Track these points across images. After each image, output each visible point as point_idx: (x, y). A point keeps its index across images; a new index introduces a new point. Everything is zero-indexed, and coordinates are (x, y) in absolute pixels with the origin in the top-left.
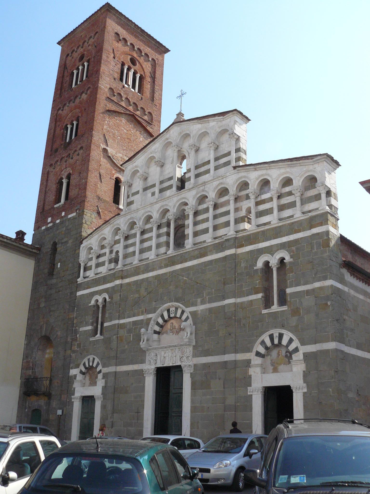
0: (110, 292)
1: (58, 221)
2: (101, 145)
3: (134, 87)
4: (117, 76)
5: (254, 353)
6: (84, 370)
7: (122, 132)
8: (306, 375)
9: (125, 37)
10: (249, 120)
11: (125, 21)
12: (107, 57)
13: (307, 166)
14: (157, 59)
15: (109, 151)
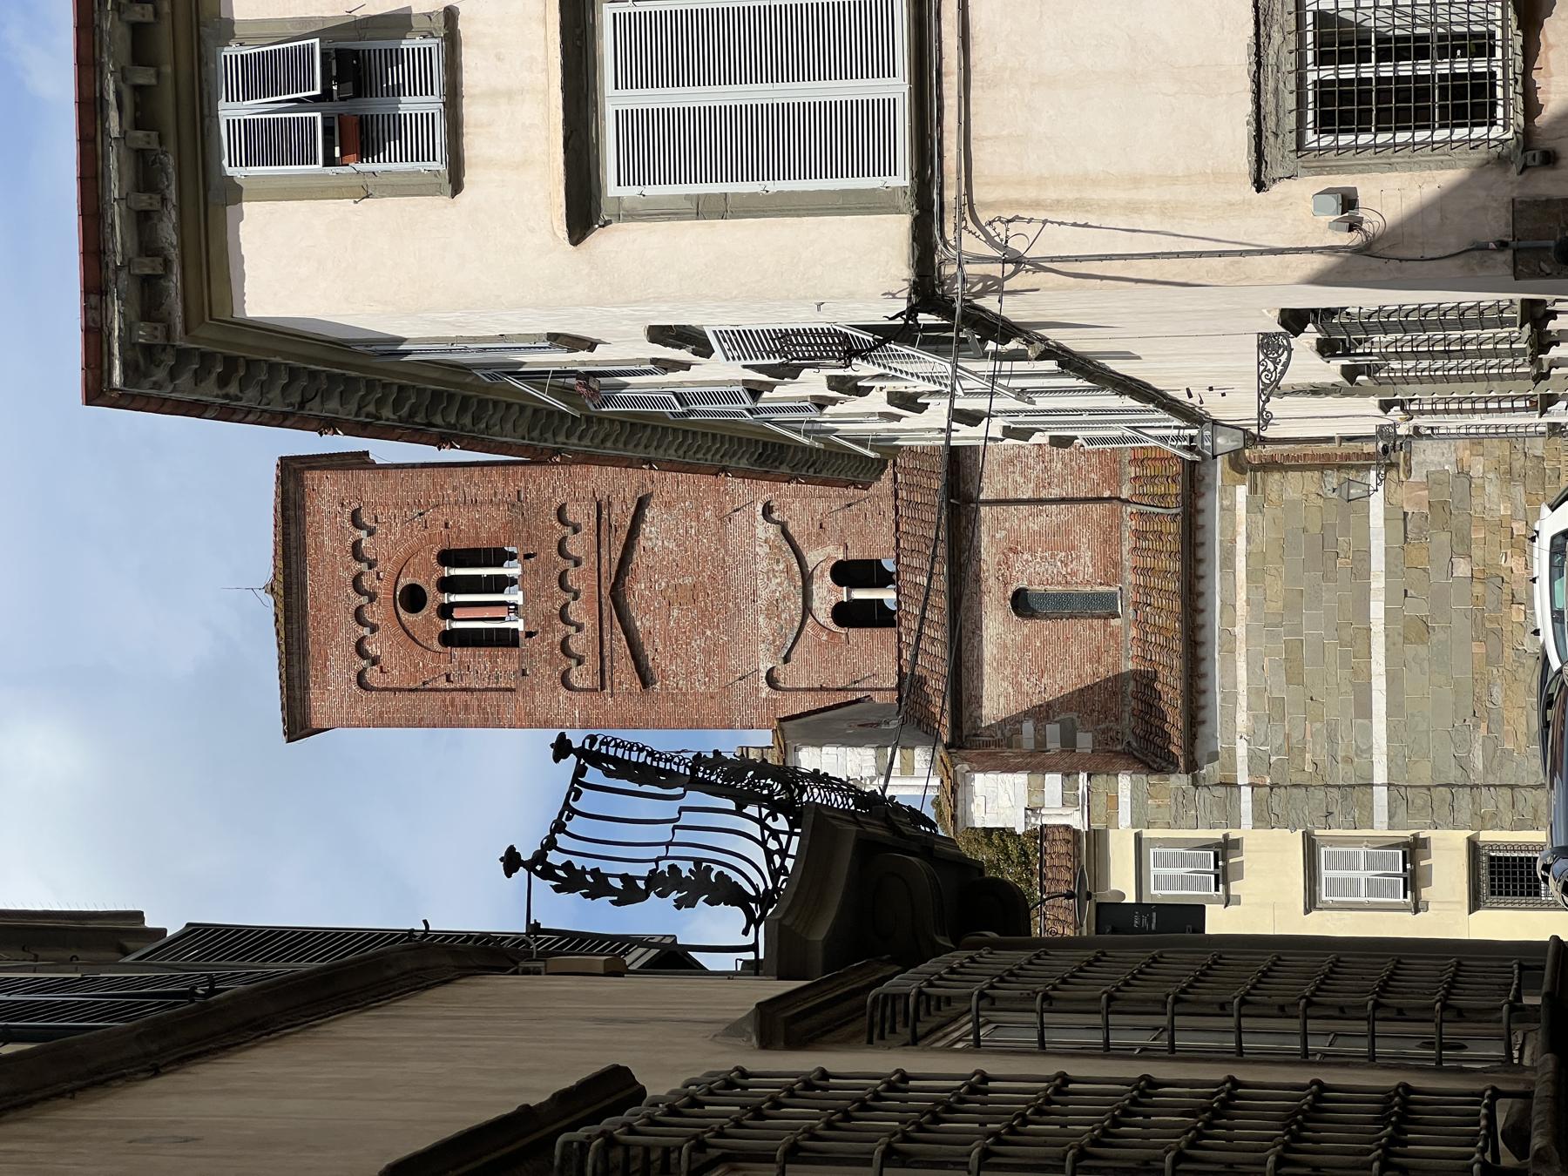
2: (764, 695)
4: (505, 662)
9: (352, 649)
15: (770, 666)
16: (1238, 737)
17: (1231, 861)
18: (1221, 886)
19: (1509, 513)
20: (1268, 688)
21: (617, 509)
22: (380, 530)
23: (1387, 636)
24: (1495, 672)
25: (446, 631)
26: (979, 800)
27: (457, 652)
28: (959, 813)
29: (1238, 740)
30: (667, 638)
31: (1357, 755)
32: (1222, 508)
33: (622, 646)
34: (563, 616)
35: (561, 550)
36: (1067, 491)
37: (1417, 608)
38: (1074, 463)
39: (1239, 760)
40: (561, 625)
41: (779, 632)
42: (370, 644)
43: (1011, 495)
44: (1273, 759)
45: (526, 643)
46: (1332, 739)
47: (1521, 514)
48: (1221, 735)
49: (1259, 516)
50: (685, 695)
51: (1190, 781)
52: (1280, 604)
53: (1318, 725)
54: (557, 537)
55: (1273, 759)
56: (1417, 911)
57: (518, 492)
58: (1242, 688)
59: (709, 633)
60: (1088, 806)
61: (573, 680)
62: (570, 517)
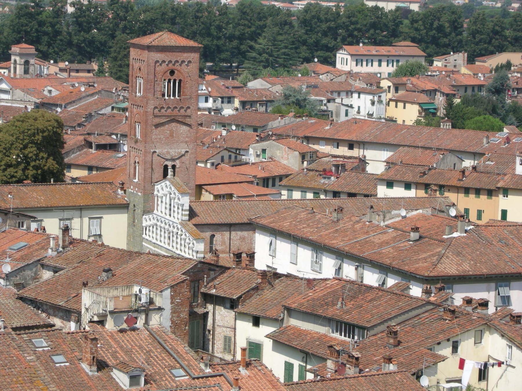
21: (189, 120)
36: (231, 244)
41: (164, 154)
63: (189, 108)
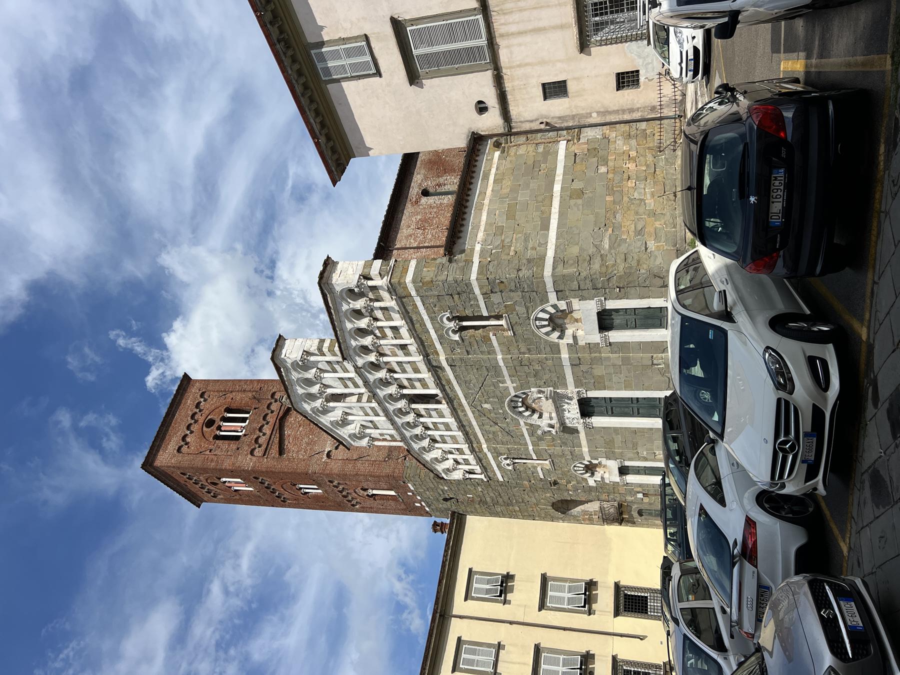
0: (497, 454)
1: (419, 498)
2: (324, 460)
3: (243, 420)
4: (233, 445)
5: (561, 341)
6: (588, 475)
7: (303, 433)
8: (582, 298)
10: (280, 336)
11: (159, 440)
12: (212, 460)
13: (336, 298)
14: (200, 390)
15: (330, 449)
16: (477, 242)
17: (509, 584)
18: (503, 595)
19: (628, 149)
20: (496, 222)
22: (209, 400)
23: (561, 197)
24: (618, 207)
25: (217, 435)
26: (338, 271)
27: (217, 442)
28: (326, 274)
29: (477, 244)
30: (295, 438)
31: (539, 246)
32: (486, 160)
33: (277, 440)
34: (260, 430)
35: (268, 407)
36: (432, 244)
37: (578, 185)
38: (436, 235)
39: (475, 252)
40: (258, 432)
42: (188, 438)
43: (408, 246)
44: (494, 251)
45: (243, 439)
46: (526, 240)
47: (635, 149)
48: (468, 243)
49: (504, 161)
50: (294, 459)
51: (447, 260)
52: (509, 190)
53: (520, 235)
54: (268, 402)
55: (494, 251)
56: (590, 614)
57: (261, 388)
58: (483, 223)
59: (311, 437)
60: (392, 273)
61: (255, 453)
62: (276, 397)
63: (273, 395)
